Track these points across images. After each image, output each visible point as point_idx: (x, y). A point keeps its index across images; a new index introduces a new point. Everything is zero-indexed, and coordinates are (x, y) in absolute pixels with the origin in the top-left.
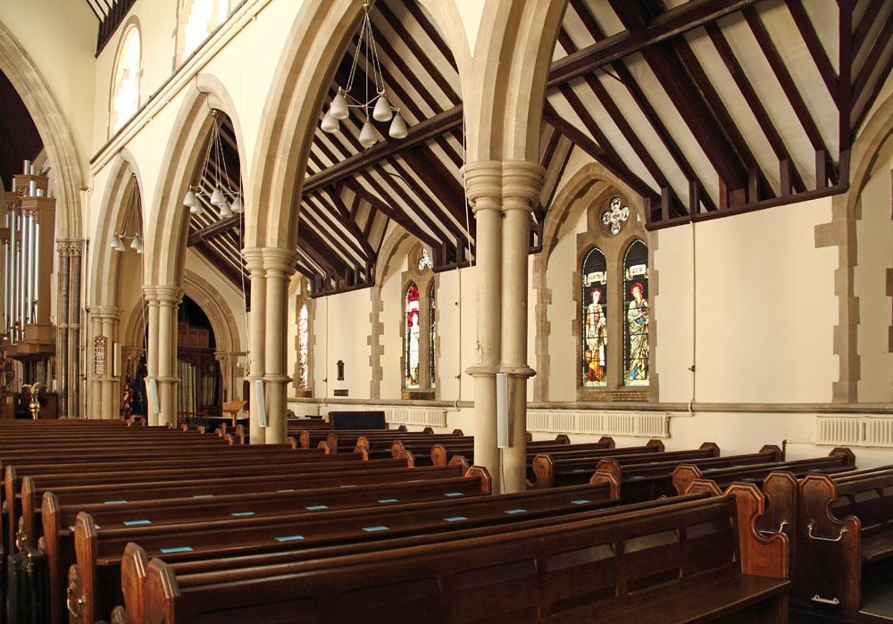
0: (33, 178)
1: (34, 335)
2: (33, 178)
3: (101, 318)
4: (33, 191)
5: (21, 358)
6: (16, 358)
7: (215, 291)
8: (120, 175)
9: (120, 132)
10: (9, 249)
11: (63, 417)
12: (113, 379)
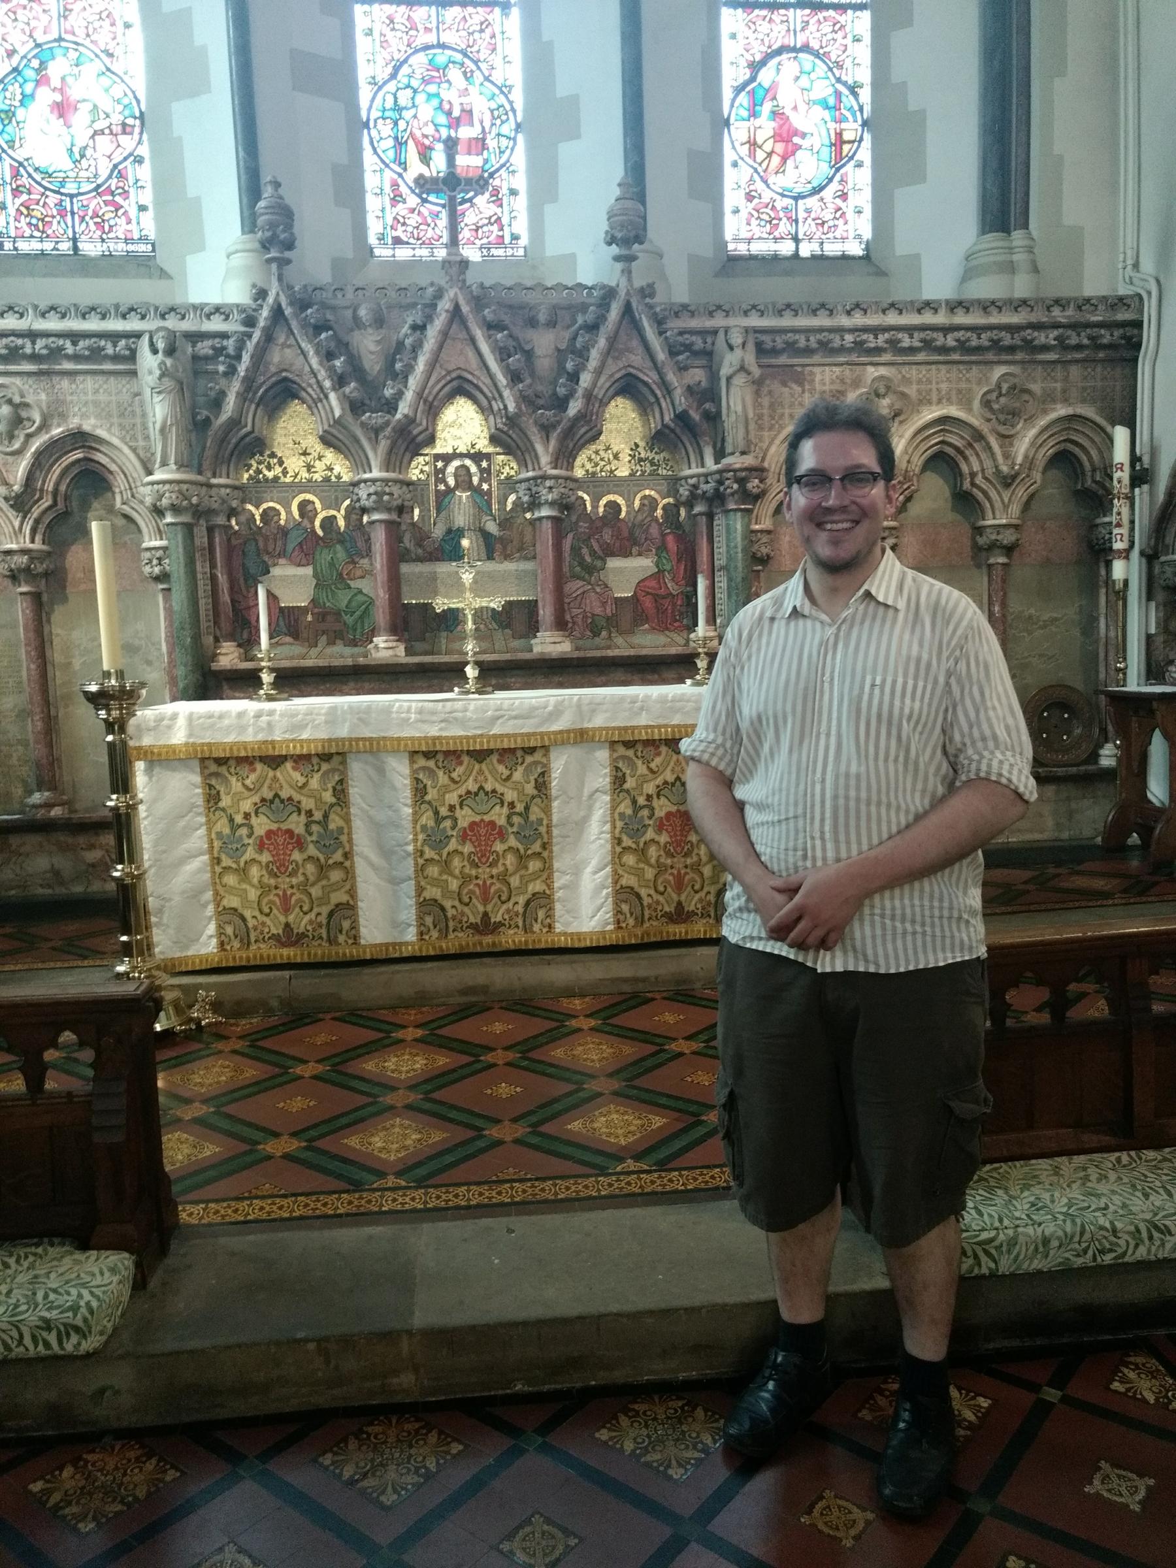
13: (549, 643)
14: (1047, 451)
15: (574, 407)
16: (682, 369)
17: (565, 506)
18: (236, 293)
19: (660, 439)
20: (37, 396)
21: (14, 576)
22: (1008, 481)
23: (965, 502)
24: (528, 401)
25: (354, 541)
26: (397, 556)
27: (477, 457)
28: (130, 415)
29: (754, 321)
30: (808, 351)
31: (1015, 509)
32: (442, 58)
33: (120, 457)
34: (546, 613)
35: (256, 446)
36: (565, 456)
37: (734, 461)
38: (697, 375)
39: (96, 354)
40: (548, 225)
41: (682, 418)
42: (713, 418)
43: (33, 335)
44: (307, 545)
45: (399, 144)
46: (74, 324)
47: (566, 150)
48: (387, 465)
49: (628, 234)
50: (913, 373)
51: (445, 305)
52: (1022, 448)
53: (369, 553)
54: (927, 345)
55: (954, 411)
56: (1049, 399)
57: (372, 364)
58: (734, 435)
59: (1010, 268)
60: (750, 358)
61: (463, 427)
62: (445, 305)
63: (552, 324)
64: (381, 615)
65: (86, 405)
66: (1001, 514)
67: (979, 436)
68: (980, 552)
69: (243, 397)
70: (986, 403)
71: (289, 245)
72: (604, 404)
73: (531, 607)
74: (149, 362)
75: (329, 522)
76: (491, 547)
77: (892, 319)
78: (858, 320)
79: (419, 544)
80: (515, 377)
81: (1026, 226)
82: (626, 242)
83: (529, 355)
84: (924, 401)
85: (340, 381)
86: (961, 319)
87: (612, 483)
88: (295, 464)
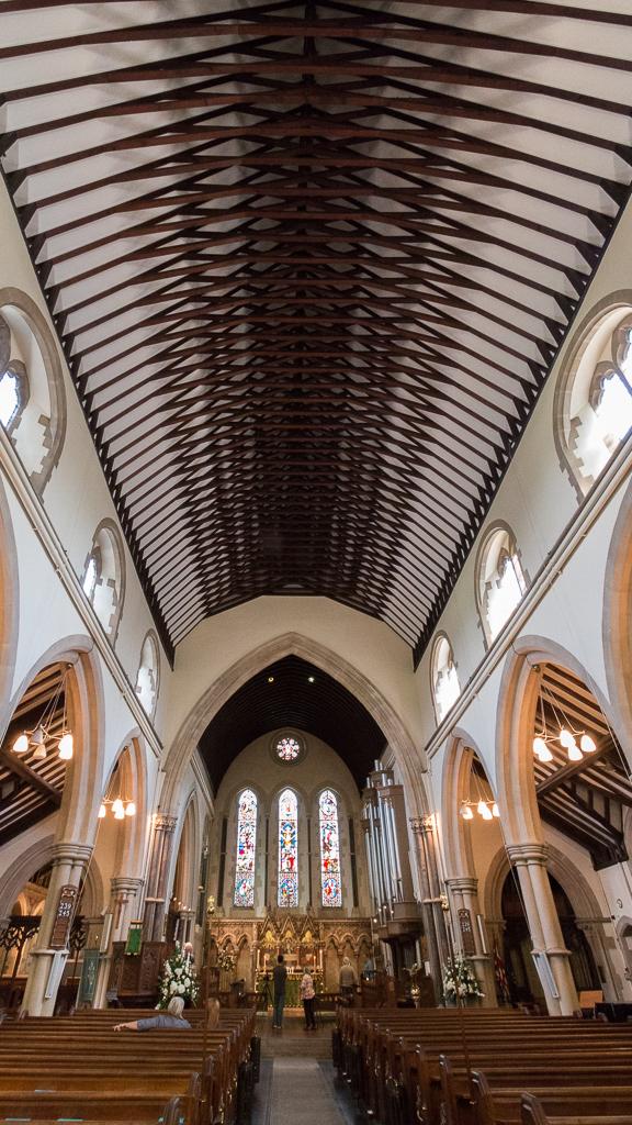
0: (383, 772)
1: (401, 914)
2: (383, 772)
3: (461, 890)
4: (385, 782)
5: (391, 940)
6: (385, 941)
7: (557, 852)
8: (454, 752)
9: (447, 716)
10: (370, 836)
11: (440, 1007)
12: (484, 958)
13: (298, 967)
18: (264, 915)
20: (241, 930)
23: (352, 947)
28: (251, 934)
40: (299, 902)
44: (269, 951)
61: (289, 934)
74: (255, 926)
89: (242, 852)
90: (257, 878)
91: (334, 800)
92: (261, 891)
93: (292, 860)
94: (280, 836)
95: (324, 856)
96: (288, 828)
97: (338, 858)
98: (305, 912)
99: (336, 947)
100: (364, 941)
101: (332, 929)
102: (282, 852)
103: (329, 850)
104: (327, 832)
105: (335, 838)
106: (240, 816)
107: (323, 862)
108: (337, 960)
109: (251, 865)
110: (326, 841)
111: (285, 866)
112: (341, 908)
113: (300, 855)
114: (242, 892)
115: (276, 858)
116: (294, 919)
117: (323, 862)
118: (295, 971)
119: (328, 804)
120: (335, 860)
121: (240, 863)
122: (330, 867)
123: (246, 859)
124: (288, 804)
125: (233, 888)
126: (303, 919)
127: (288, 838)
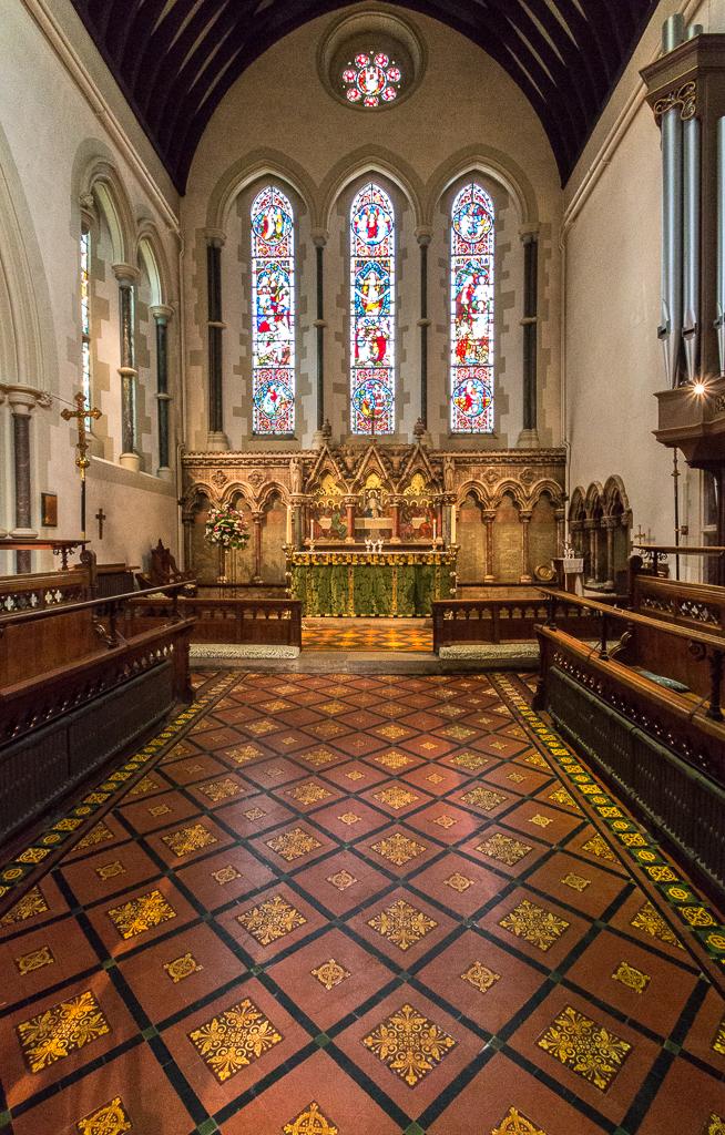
13: (395, 541)
14: (540, 490)
15: (404, 477)
16: (433, 467)
17: (399, 503)
18: (316, 447)
19: (428, 485)
20: (264, 474)
21: (254, 520)
22: (528, 499)
23: (516, 505)
24: (391, 475)
25: (343, 512)
26: (354, 516)
27: (377, 490)
28: (287, 480)
29: (454, 455)
30: (469, 463)
31: (530, 507)
32: (373, 382)
33: (284, 489)
34: (394, 532)
35: (319, 486)
36: (401, 490)
37: (448, 492)
38: (438, 469)
39: (280, 463)
40: (399, 425)
41: (433, 480)
42: (442, 481)
43: (265, 459)
45: (361, 404)
46: (275, 456)
47: (405, 406)
48: (353, 492)
49: (422, 428)
50: (500, 468)
51: (370, 450)
52: (531, 490)
53: (346, 515)
54: (504, 461)
55: (512, 479)
56: (540, 476)
57: (350, 466)
58: (447, 486)
59: (530, 439)
60: (453, 467)
61: (374, 481)
62: (370, 450)
63: (398, 455)
64: (349, 532)
65: (276, 475)
66: (526, 508)
67: (519, 486)
68: (521, 519)
69: (316, 474)
70: (521, 477)
71: (330, 435)
72: (412, 477)
73: (390, 530)
74: (293, 465)
75: (336, 507)
76: (380, 514)
77: (494, 454)
78: (484, 454)
79: (359, 512)
80: (388, 469)
81: (535, 427)
82: (419, 435)
83: (392, 463)
84: (503, 476)
85: (341, 470)
86: (513, 454)
87: (414, 497)
88: (328, 491)
89: (264, 328)
90: (302, 379)
91: (490, 208)
92: (311, 402)
93: (381, 342)
94: (353, 290)
95: (457, 332)
96: (372, 276)
97: (491, 336)
98: (411, 439)
99: (480, 505)
100: (545, 493)
101: (474, 469)
102: (356, 326)
103: (470, 320)
104: (470, 280)
105: (485, 293)
106: (256, 249)
107: (454, 346)
108: (482, 529)
109: (286, 353)
110: (464, 300)
111: (365, 354)
112: (493, 435)
113: (401, 330)
114: (268, 407)
115: (343, 338)
116: (386, 453)
117: (454, 346)
118: (385, 548)
119: (472, 221)
120: (484, 341)
121: (261, 349)
122: (470, 356)
123: (275, 342)
124: (372, 219)
125: (249, 401)
126: (407, 453)
127: (373, 296)
